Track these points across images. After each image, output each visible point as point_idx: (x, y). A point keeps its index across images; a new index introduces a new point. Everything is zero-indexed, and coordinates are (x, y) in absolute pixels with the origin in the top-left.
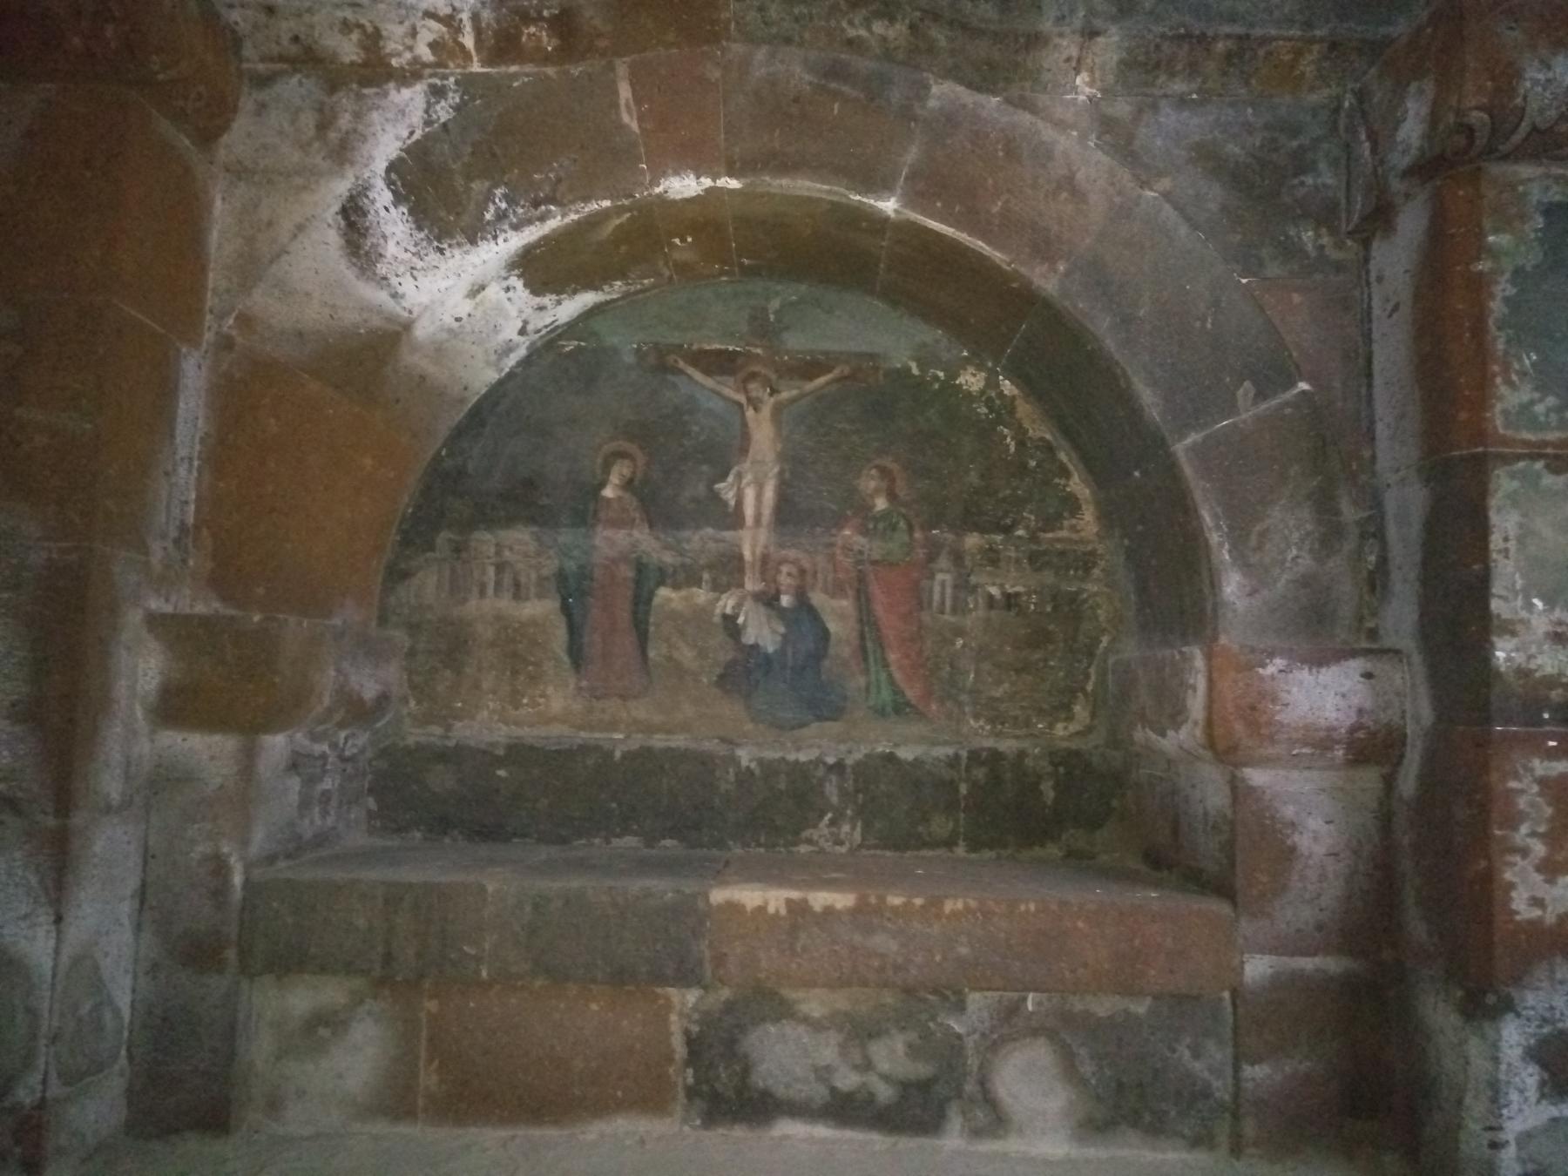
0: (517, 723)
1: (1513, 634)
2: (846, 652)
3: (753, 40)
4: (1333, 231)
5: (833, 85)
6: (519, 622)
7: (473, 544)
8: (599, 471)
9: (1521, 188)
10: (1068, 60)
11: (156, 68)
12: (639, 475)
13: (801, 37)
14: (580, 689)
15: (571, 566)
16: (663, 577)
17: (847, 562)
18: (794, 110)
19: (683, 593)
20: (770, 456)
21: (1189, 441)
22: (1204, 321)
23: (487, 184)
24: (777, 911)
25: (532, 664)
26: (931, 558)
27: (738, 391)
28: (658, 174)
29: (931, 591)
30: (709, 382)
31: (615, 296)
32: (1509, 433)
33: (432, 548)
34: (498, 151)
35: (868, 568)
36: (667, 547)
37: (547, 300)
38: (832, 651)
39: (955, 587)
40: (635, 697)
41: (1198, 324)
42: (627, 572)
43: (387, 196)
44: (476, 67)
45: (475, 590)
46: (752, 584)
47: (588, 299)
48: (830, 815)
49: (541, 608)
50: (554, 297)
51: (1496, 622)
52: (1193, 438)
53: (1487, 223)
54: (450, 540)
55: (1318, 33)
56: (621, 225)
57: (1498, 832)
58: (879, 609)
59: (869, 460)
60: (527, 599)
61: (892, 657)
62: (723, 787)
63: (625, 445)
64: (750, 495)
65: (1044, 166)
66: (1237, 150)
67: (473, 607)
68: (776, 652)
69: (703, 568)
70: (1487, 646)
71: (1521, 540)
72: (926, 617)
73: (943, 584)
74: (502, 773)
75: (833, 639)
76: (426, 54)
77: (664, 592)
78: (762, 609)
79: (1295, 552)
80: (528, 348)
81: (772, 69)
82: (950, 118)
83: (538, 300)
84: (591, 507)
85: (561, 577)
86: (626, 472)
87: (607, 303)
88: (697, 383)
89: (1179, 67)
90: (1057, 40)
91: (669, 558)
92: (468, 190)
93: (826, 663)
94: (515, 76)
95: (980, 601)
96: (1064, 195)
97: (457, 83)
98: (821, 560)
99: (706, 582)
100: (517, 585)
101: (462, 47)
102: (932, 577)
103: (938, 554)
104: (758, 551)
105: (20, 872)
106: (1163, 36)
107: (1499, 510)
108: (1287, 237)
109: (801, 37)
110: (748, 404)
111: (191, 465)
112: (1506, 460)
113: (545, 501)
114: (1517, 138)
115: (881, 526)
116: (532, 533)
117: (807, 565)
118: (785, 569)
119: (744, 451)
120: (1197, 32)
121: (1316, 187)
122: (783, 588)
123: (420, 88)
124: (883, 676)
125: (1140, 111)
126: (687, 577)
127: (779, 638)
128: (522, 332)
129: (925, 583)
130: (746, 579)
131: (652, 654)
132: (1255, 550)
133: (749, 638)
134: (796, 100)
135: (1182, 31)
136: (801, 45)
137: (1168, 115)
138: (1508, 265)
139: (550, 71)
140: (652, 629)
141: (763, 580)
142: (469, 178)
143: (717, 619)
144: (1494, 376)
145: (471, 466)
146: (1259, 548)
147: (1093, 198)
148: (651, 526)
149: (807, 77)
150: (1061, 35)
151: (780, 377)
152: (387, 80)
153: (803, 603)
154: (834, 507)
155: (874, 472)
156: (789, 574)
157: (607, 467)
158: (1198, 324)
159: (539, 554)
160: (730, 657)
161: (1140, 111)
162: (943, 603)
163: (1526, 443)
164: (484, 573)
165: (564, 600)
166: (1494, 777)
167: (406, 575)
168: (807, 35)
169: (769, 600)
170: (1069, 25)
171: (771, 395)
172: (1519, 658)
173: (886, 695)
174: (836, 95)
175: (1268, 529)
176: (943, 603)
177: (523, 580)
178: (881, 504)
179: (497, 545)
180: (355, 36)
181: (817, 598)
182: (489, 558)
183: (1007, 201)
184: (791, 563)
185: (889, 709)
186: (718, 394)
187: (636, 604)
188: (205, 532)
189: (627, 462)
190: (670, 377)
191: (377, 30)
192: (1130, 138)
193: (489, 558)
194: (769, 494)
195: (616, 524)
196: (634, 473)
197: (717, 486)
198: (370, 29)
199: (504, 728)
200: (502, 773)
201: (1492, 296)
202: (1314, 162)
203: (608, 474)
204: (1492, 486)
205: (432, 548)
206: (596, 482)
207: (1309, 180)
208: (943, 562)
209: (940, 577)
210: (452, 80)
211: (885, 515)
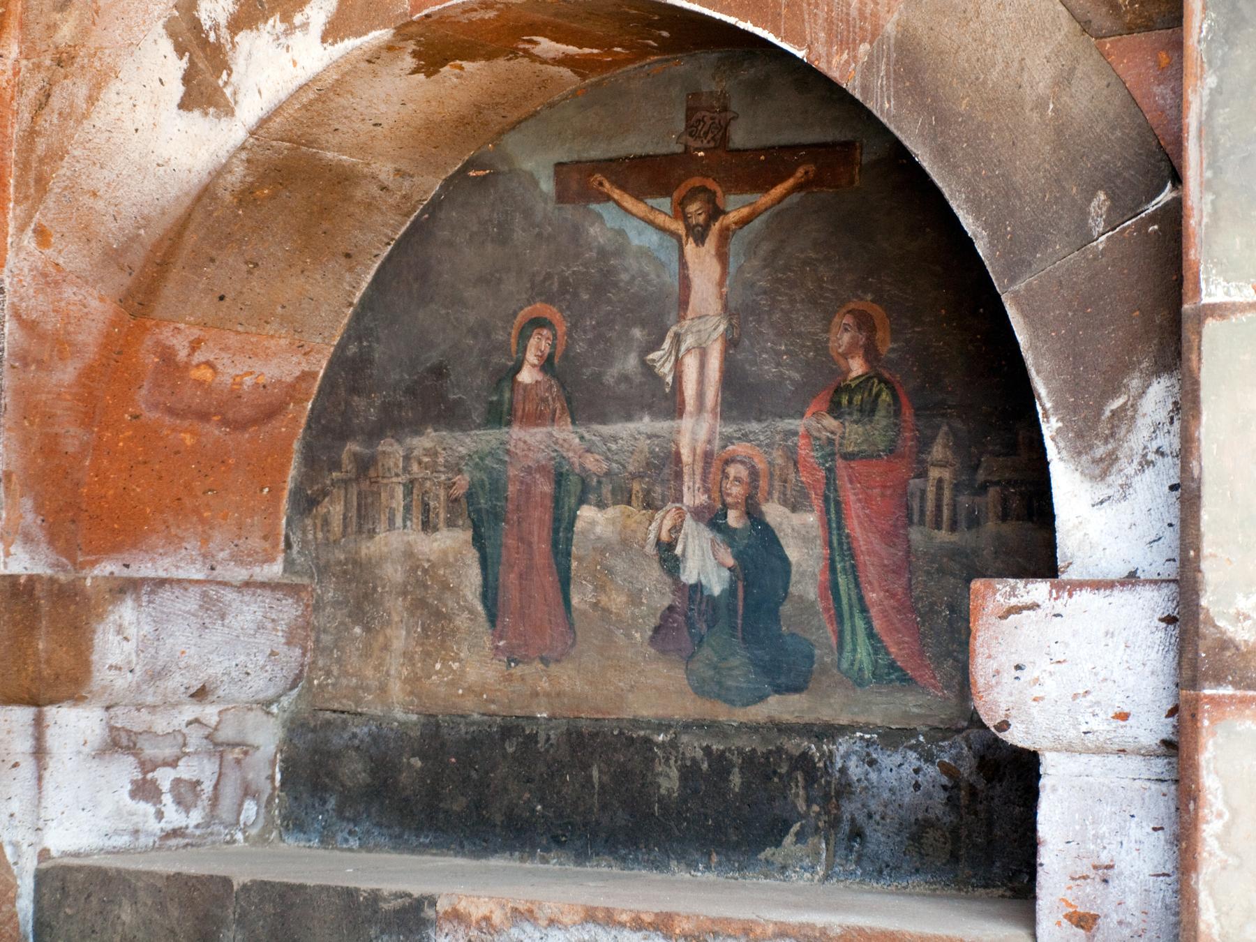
6: (428, 561)
12: (560, 349)
14: (497, 648)
19: (612, 512)
20: (714, 306)
27: (676, 217)
35: (840, 462)
38: (793, 589)
39: (957, 488)
40: (558, 661)
42: (545, 487)
46: (693, 496)
54: (355, 454)
58: (855, 527)
59: (843, 303)
60: (435, 529)
61: (872, 596)
62: (665, 784)
63: (539, 308)
68: (723, 591)
73: (940, 481)
75: (794, 569)
77: (587, 513)
78: (708, 534)
86: (545, 346)
91: (593, 463)
99: (637, 498)
100: (426, 509)
102: (923, 474)
103: (933, 439)
104: (699, 451)
110: (687, 236)
115: (857, 398)
117: (761, 466)
119: (684, 303)
122: (729, 500)
124: (860, 624)
127: (726, 574)
130: (685, 489)
131: (575, 600)
133: (689, 575)
140: (574, 564)
143: (650, 549)
146: (1112, 435)
148: (573, 423)
151: (727, 192)
154: (797, 376)
155: (848, 320)
156: (736, 479)
157: (524, 337)
160: (666, 603)
162: (939, 507)
165: (476, 528)
169: (714, 519)
173: (863, 653)
178: (857, 367)
181: (774, 512)
182: (397, 475)
184: (742, 462)
185: (867, 674)
187: (556, 531)
189: (545, 332)
190: (594, 206)
195: (535, 419)
196: (553, 346)
197: (651, 356)
205: (336, 465)
206: (511, 364)
209: (934, 473)
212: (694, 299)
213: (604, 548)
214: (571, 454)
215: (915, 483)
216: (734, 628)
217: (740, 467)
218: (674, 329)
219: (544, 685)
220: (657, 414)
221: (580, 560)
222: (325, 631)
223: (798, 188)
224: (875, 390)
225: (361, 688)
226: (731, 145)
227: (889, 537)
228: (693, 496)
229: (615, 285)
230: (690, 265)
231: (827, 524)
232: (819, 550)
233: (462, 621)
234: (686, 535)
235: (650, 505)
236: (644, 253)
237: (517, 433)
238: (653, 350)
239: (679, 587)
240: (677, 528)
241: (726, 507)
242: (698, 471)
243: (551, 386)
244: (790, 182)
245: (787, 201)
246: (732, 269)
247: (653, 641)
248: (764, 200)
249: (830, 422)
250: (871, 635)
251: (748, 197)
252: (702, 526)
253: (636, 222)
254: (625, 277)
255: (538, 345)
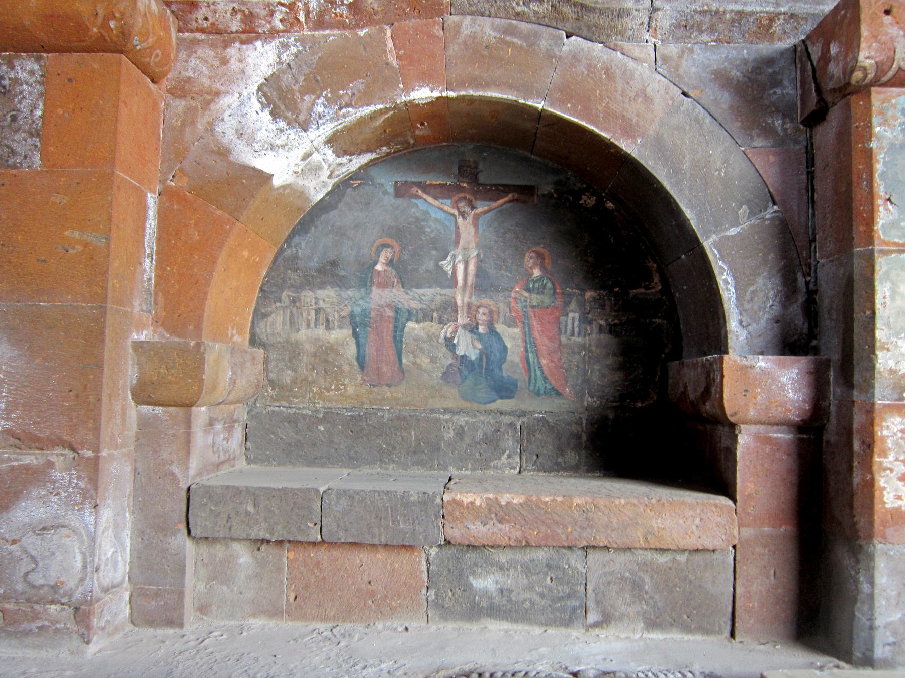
0: (330, 401)
1: (888, 350)
2: (517, 359)
3: (463, 13)
4: (792, 120)
5: (508, 38)
6: (329, 342)
7: (302, 298)
8: (373, 255)
9: (894, 101)
10: (642, 23)
11: (137, 42)
13: (490, 12)
15: (358, 310)
16: (410, 315)
17: (519, 307)
18: (485, 53)
19: (422, 325)
21: (711, 240)
22: (720, 171)
23: (313, 97)
24: (481, 505)
25: (338, 367)
26: (567, 304)
28: (408, 89)
29: (566, 324)
30: (436, 203)
31: (382, 155)
32: (887, 239)
33: (280, 301)
34: (319, 78)
36: (414, 299)
37: (344, 160)
38: (508, 358)
39: (580, 320)
41: (717, 173)
42: (390, 313)
43: (257, 106)
44: (307, 32)
45: (304, 325)
46: (462, 319)
47: (366, 158)
48: (507, 452)
49: (341, 335)
50: (348, 157)
51: (878, 344)
52: (714, 237)
53: (875, 120)
54: (289, 296)
55: (783, 9)
56: (388, 117)
57: (878, 459)
58: (536, 334)
59: (529, 248)
63: (388, 240)
64: (460, 268)
65: (628, 83)
66: (738, 74)
67: (303, 334)
68: (476, 358)
69: (433, 311)
70: (872, 356)
71: (893, 298)
72: (563, 339)
73: (573, 319)
74: (322, 428)
75: (509, 350)
76: (280, 26)
77: (410, 325)
78: (468, 335)
79: (771, 303)
80: (334, 185)
81: (473, 30)
82: (575, 57)
83: (339, 160)
84: (369, 276)
85: (352, 316)
87: (377, 159)
88: (429, 203)
89: (704, 27)
90: (635, 13)
91: (415, 305)
92: (303, 100)
93: (504, 366)
94: (329, 36)
95: (594, 328)
96: (640, 99)
97: (296, 40)
98: (502, 306)
100: (328, 321)
101: (298, 20)
102: (567, 315)
103: (570, 303)
104: (465, 302)
105: (76, 481)
106: (695, 11)
107: (881, 283)
108: (767, 123)
109: (490, 12)
111: (152, 258)
112: (883, 252)
113: (342, 273)
114: (891, 74)
115: (537, 285)
116: (336, 291)
117: (494, 309)
118: (481, 310)
119: (457, 242)
120: (714, 9)
121: (783, 95)
122: (480, 322)
123: (276, 42)
124: (539, 373)
125: (683, 52)
126: (425, 316)
128: (330, 177)
129: (562, 319)
130: (459, 317)
131: (404, 361)
132: (748, 302)
133: (460, 351)
134: (487, 47)
135: (706, 8)
136: (490, 16)
137: (699, 54)
138: (885, 143)
139: (347, 33)
140: (404, 346)
141: (468, 317)
142: (304, 92)
143: (442, 340)
144: (879, 206)
145: (300, 253)
146: (752, 300)
147: (657, 101)
148: (403, 287)
149: (493, 34)
150: (637, 10)
151: (476, 199)
152: (257, 39)
153: (492, 331)
155: (533, 254)
157: (378, 253)
158: (717, 173)
159: (339, 304)
160: (449, 362)
161: (683, 52)
162: (573, 328)
163: (895, 244)
164: (309, 315)
166: (877, 428)
167: (265, 316)
168: (493, 11)
169: (472, 329)
170: (642, 4)
171: (472, 210)
172: (891, 364)
174: (509, 44)
175: (756, 290)
176: (573, 331)
177: (331, 319)
178: (537, 273)
179: (316, 298)
180: (239, 16)
181: (500, 328)
182: (311, 306)
183: (608, 103)
185: (542, 392)
186: (442, 209)
187: (395, 332)
188: (161, 294)
189: (389, 249)
190: (414, 201)
191: (251, 13)
192: (677, 68)
193: (311, 306)
194: (472, 267)
195: (383, 286)
196: (393, 256)
197: (441, 263)
198: (247, 12)
199: (321, 402)
200: (322, 428)
201: (878, 162)
202: (781, 81)
203: (379, 256)
204: (877, 267)
205: (280, 301)
207: (779, 91)
208: (573, 305)
209: (571, 315)
210: (293, 39)
211: (540, 279)
212: (461, 242)
213: (417, 339)
214: (402, 300)
215: (562, 319)
216: (481, 373)
217: (485, 309)
218: (452, 252)
219: (388, 394)
220: (442, 287)
221: (406, 344)
222: (271, 372)
223: (510, 201)
224: (544, 282)
225: (291, 396)
226: (479, 182)
227: (551, 339)
228: (462, 319)
229: (424, 232)
230: (460, 227)
231: (524, 334)
232: (520, 342)
233: (346, 368)
234: (459, 336)
235: (441, 322)
236: (436, 220)
237: (375, 291)
238: (442, 260)
239: (455, 356)
240: (455, 332)
241: (477, 324)
242: (465, 310)
243: (392, 273)
244: (506, 199)
245: (504, 207)
246: (480, 231)
247: (442, 378)
248: (494, 205)
249: (526, 294)
250: (545, 378)
251: (487, 203)
252: (467, 332)
253: (434, 208)
254: (428, 230)
255: (385, 255)
